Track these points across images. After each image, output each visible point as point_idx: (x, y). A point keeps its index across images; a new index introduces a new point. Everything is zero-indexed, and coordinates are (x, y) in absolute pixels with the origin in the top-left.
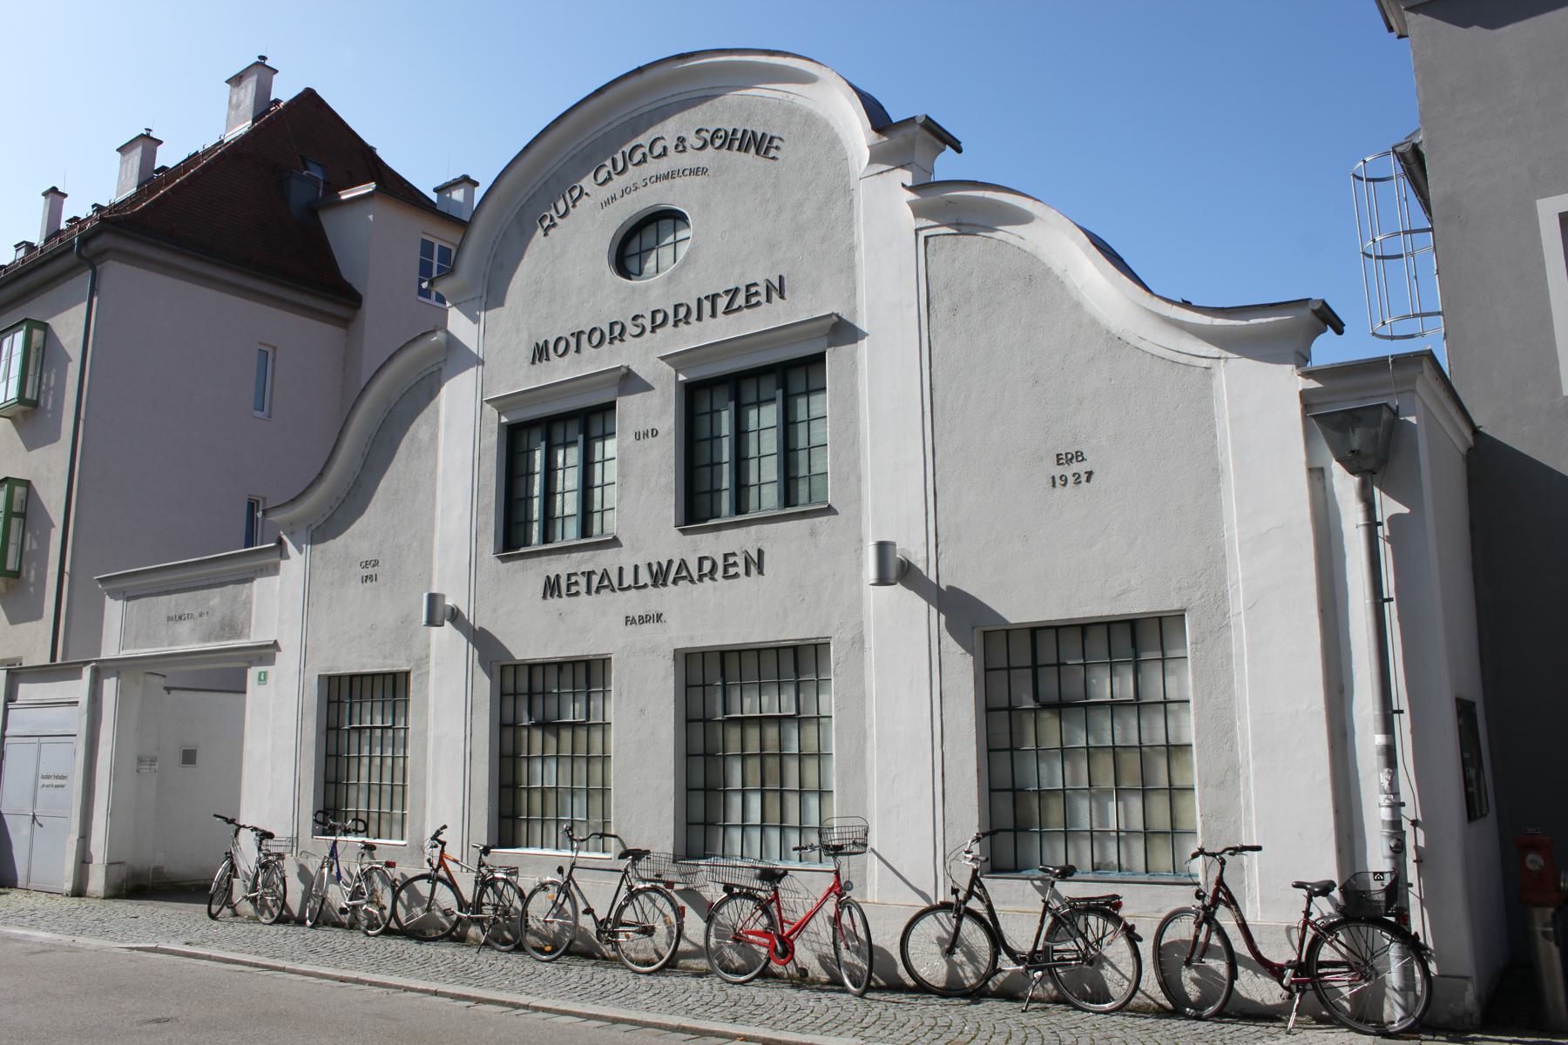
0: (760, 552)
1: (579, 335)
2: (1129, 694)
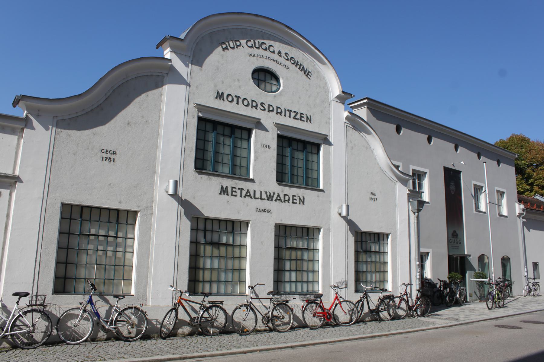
0: (304, 198)
2: (377, 250)
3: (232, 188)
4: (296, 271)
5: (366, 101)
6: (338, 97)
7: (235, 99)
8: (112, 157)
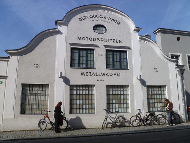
1: (87, 38)
2: (160, 93)
3: (86, 73)
4: (118, 103)
5: (159, 29)
6: (135, 30)
7: (86, 39)
8: (39, 66)
